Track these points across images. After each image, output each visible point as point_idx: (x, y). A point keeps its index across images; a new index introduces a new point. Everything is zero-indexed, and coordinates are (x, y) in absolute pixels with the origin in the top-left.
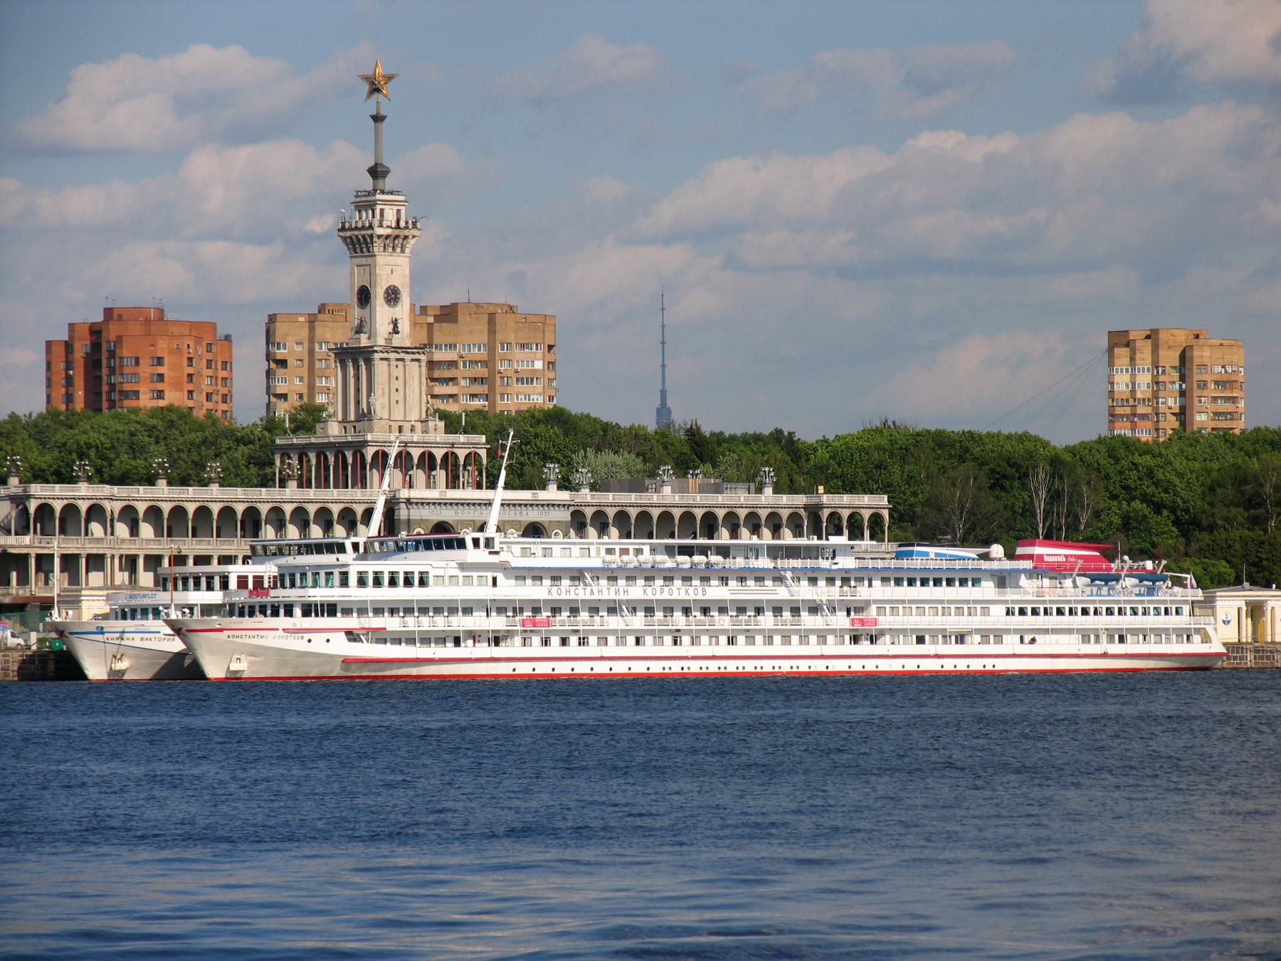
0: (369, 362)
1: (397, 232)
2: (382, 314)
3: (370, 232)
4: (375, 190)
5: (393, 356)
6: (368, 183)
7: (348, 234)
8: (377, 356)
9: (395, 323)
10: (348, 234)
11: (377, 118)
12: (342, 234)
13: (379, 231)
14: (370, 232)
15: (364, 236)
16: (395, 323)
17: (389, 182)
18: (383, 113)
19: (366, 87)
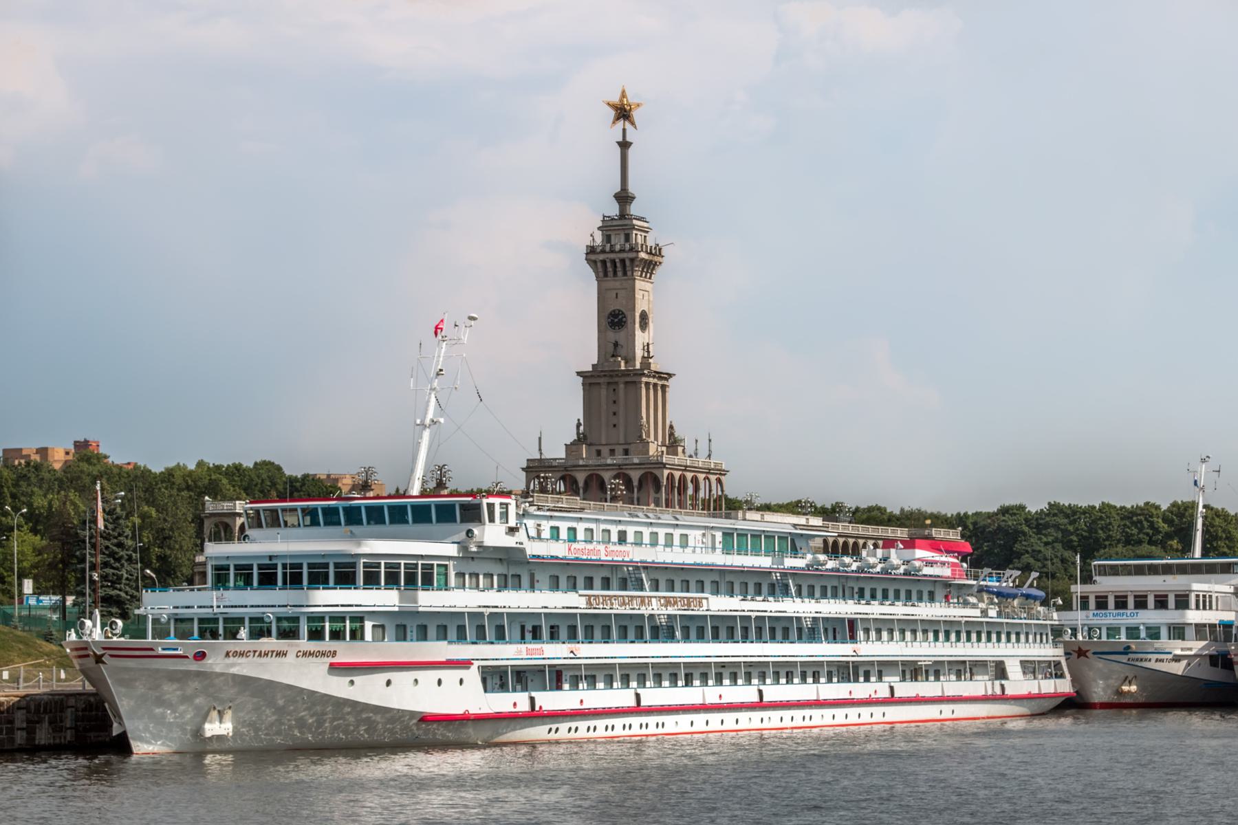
0: (636, 384)
1: (651, 258)
2: (640, 338)
3: (632, 255)
4: (623, 215)
5: (652, 380)
6: (613, 210)
7: (602, 257)
8: (644, 379)
9: (647, 347)
10: (602, 257)
11: (624, 145)
12: (593, 257)
13: (643, 255)
14: (632, 255)
15: (623, 261)
16: (647, 347)
17: (634, 209)
18: (628, 139)
19: (612, 113)
